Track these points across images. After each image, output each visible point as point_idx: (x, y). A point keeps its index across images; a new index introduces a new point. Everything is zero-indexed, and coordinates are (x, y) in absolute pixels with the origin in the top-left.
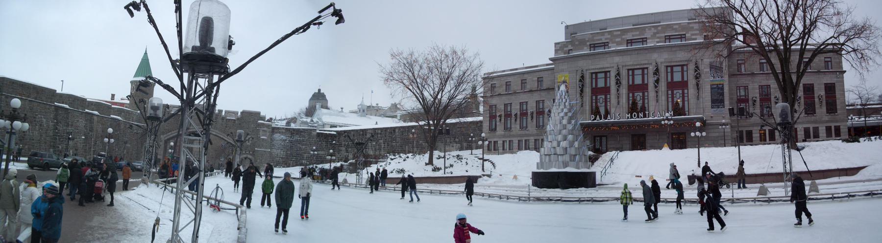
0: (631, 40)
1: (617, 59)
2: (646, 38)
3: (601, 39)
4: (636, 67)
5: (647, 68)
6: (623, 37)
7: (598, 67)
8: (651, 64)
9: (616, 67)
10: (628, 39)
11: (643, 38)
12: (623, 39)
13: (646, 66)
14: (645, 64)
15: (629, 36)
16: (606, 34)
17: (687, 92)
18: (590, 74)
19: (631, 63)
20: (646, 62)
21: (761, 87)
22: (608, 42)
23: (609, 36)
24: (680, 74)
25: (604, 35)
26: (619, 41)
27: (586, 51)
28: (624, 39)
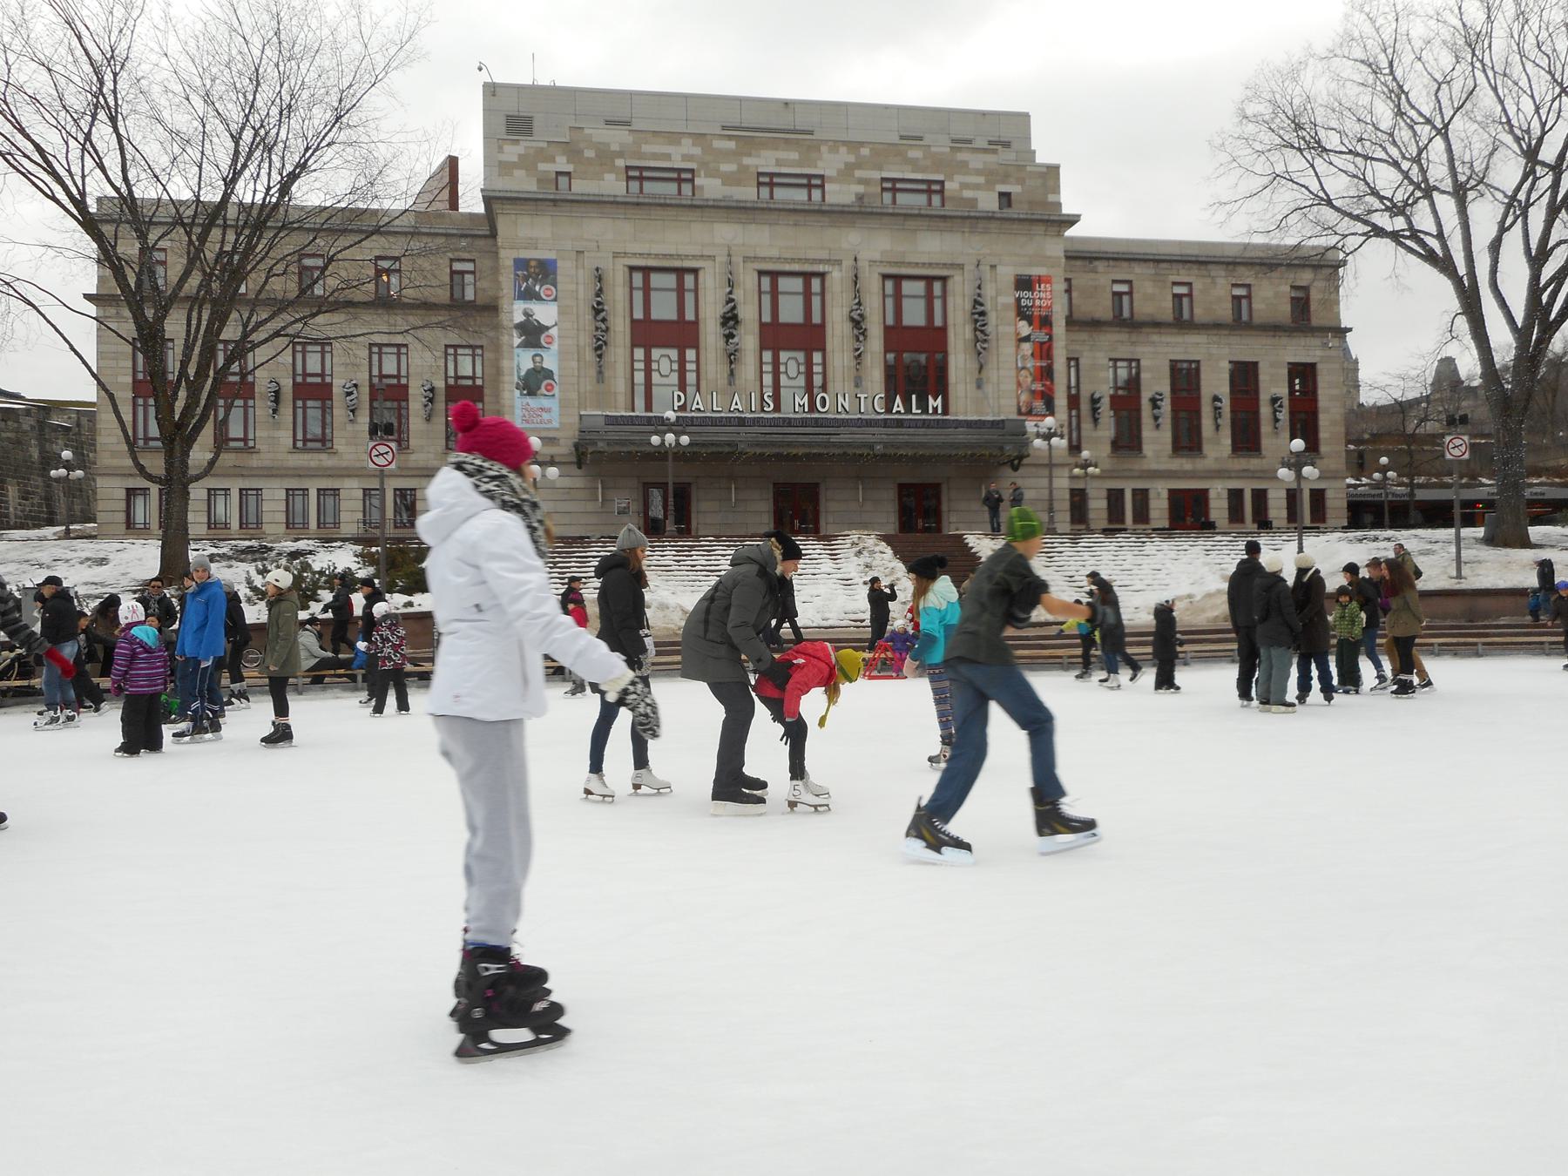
0: (772, 175)
1: (726, 233)
2: (822, 177)
3: (668, 157)
4: (787, 268)
5: (822, 275)
6: (747, 161)
7: (656, 249)
8: (839, 262)
9: (722, 259)
10: (760, 170)
11: (809, 177)
12: (743, 169)
13: (821, 268)
14: (821, 261)
15: (766, 161)
16: (686, 142)
17: (820, 361)
18: (627, 270)
19: (774, 253)
20: (824, 255)
21: (1175, 367)
22: (692, 171)
23: (697, 151)
24: (922, 303)
25: (679, 143)
26: (732, 173)
27: (612, 185)
28: (748, 167)
